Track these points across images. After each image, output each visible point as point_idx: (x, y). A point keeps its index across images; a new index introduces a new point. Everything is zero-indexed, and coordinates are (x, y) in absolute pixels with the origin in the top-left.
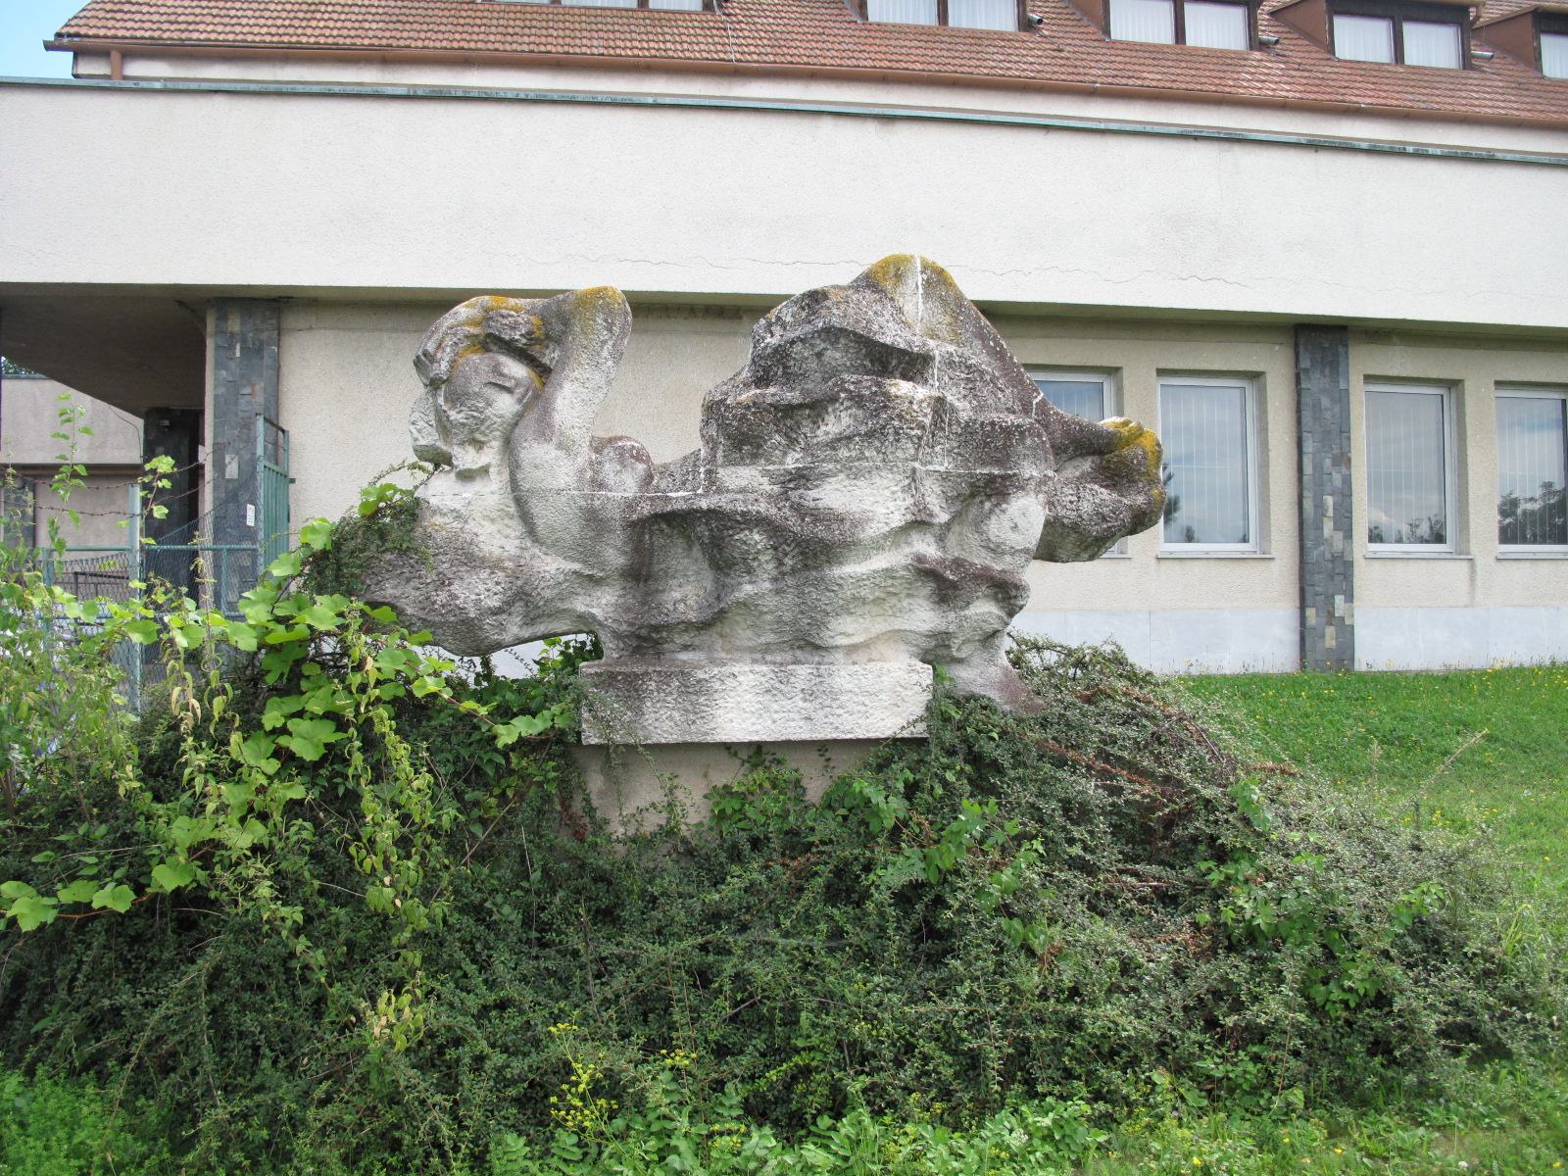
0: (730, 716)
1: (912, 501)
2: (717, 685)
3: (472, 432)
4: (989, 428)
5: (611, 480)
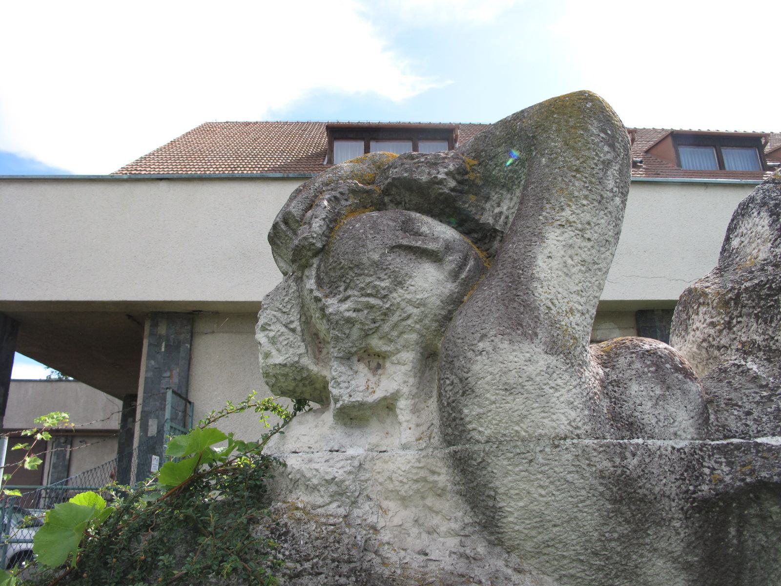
5: (648, 413)
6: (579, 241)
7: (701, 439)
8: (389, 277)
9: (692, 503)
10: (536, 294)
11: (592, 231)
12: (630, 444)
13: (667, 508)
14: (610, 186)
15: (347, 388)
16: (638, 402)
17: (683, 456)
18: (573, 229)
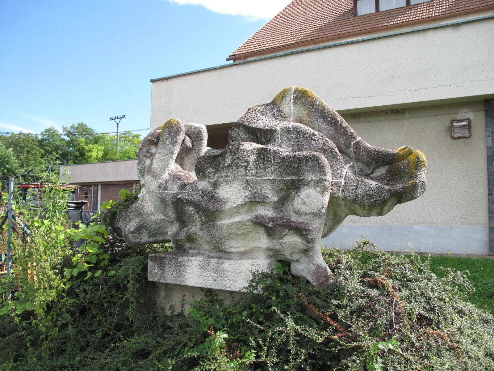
0: (190, 276)
1: (249, 193)
2: (186, 264)
4: (292, 159)
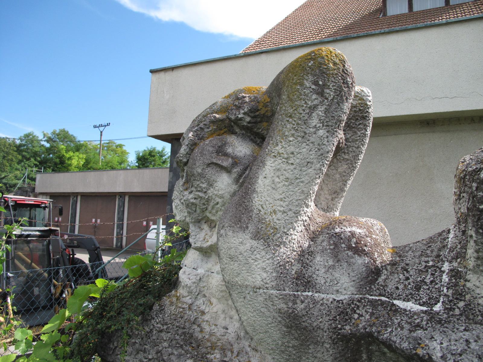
3: (203, 211)
6: (284, 166)
7: (361, 294)
8: (206, 182)
9: (337, 336)
10: (254, 202)
11: (294, 158)
12: (302, 295)
13: (321, 336)
14: (314, 124)
15: (194, 239)
16: (317, 268)
17: (340, 305)
18: (281, 158)
